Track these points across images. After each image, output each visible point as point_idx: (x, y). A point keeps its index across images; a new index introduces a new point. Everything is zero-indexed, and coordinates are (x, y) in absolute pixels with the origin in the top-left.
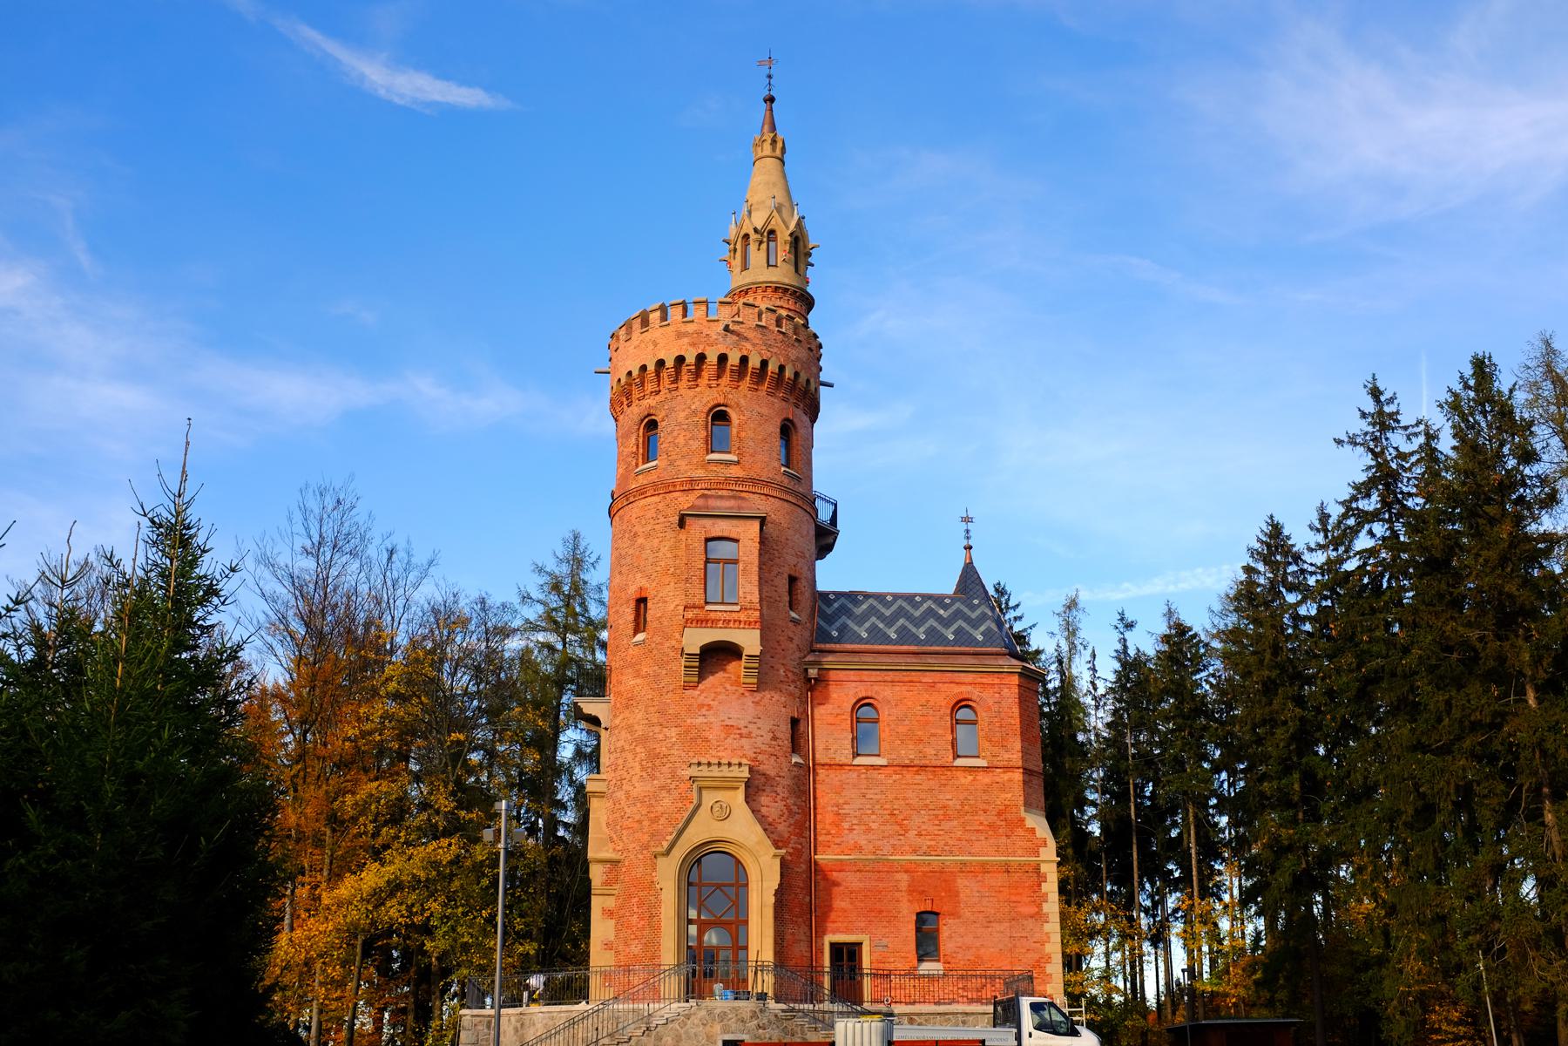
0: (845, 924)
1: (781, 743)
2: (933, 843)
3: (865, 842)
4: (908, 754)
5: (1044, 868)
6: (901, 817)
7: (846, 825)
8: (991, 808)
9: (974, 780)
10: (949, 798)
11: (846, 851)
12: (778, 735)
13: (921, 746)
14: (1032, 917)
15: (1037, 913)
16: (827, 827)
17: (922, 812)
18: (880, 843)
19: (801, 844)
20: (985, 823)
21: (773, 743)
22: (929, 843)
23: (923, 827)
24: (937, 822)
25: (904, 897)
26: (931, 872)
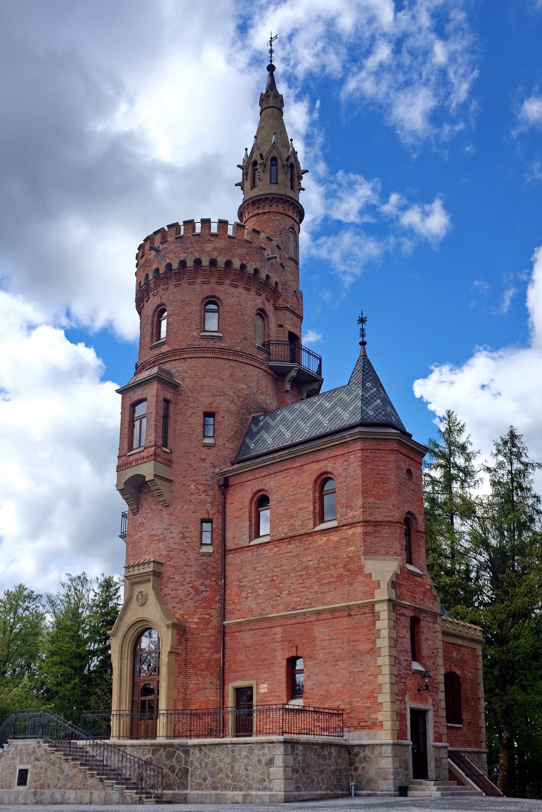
0: (242, 673)
1: (189, 540)
2: (298, 599)
3: (255, 606)
4: (284, 530)
5: (378, 608)
6: (278, 582)
7: (244, 595)
8: (339, 562)
9: (328, 540)
10: (311, 560)
11: (244, 615)
12: (187, 535)
13: (292, 521)
14: (368, 653)
15: (372, 649)
16: (233, 597)
17: (292, 575)
18: (264, 605)
19: (209, 614)
20: (335, 575)
21: (182, 541)
22: (295, 600)
23: (292, 587)
24: (301, 581)
25: (278, 646)
26: (297, 623)
